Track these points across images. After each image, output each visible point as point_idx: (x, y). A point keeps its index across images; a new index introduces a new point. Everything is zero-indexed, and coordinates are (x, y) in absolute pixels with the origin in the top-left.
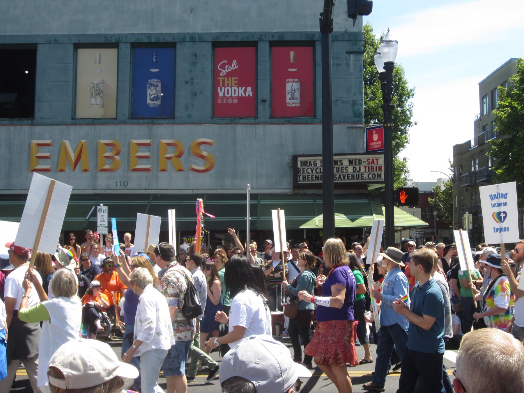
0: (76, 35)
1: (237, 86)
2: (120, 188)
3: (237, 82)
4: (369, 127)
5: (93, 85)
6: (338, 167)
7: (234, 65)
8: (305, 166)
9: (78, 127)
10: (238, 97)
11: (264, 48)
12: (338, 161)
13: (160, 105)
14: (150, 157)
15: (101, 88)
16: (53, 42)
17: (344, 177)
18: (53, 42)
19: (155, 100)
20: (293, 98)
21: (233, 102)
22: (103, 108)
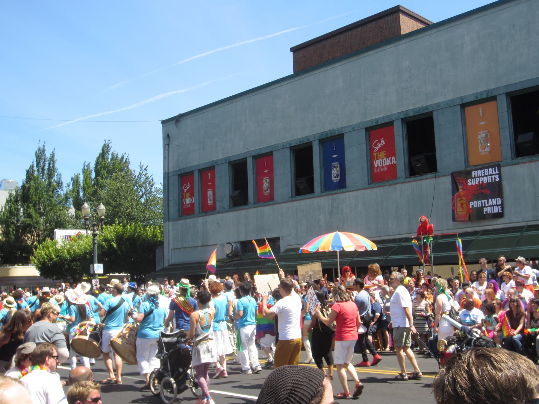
1: (385, 157)
3: (385, 154)
13: (340, 180)
20: (210, 200)
21: (384, 171)
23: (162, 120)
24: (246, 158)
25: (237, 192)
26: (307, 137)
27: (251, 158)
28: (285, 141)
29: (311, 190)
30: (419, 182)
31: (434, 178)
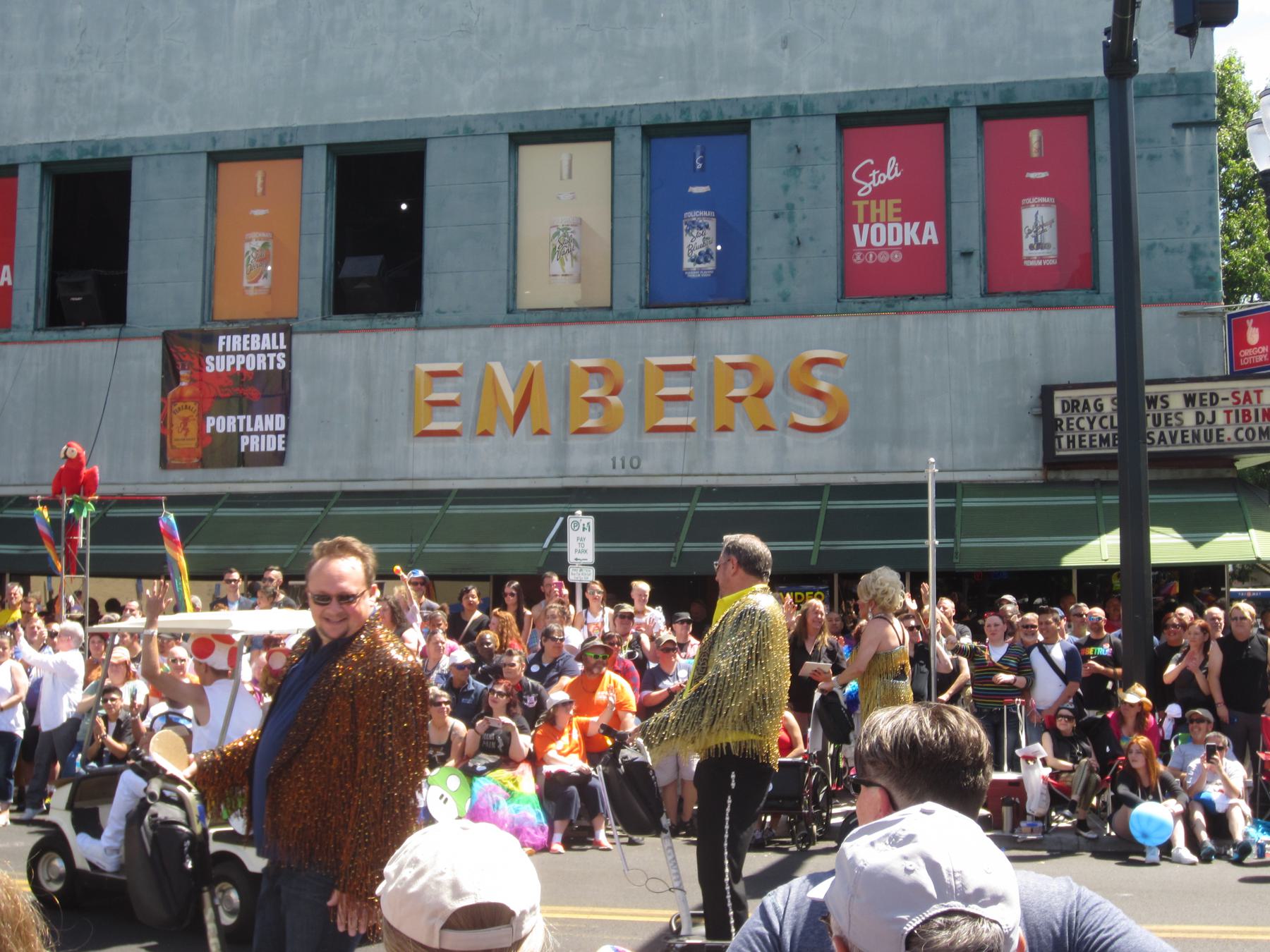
1: (900, 219)
2: (623, 472)
3: (899, 210)
4: (1233, 312)
5: (555, 230)
6: (1156, 413)
7: (893, 170)
8: (1073, 411)
9: (522, 331)
10: (903, 248)
11: (964, 124)
12: (1156, 397)
13: (716, 273)
14: (692, 396)
15: (573, 236)
16: (461, 132)
17: (1173, 439)
18: (461, 132)
19: (702, 260)
20: (1040, 246)
21: (890, 262)
22: (579, 285)
31: (409, 328)
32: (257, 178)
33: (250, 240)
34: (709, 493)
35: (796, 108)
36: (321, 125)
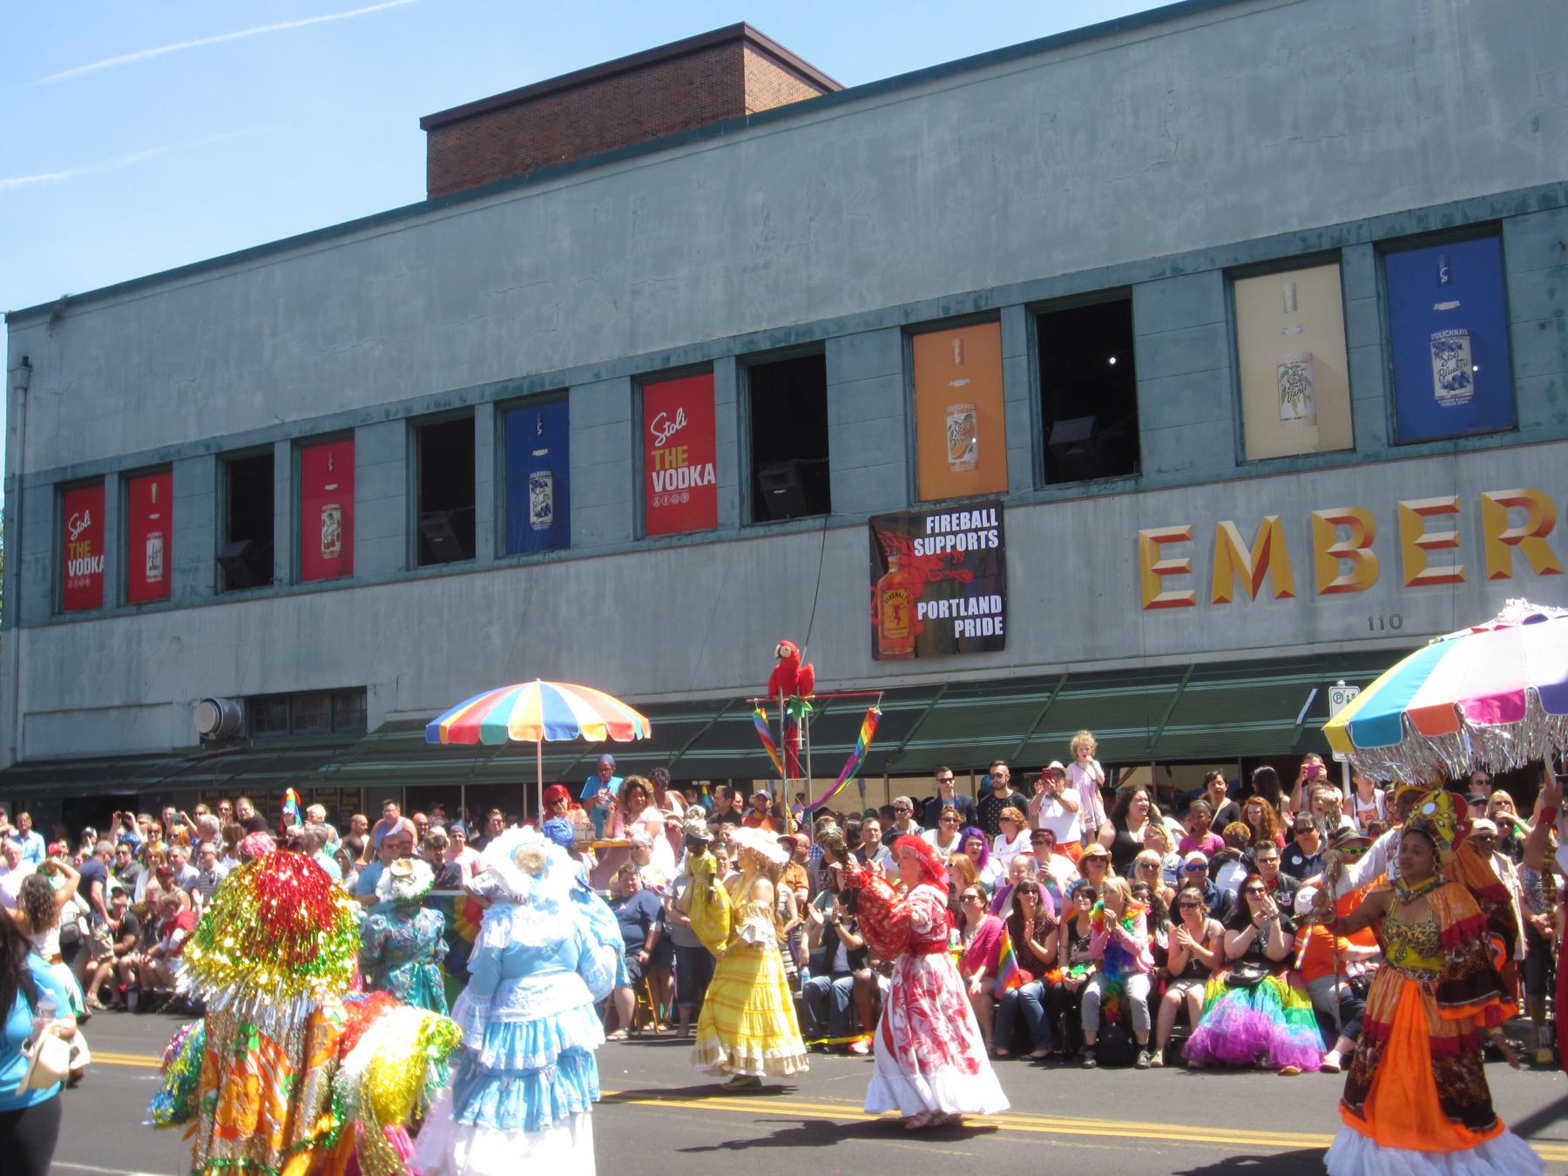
0: (1229, 246)
1: (686, 464)
2: (1382, 633)
3: (685, 456)
5: (1282, 369)
7: (681, 420)
9: (1253, 483)
20: (154, 567)
23: (7, 311)
24: (271, 445)
25: (241, 546)
26: (461, 393)
27: (288, 445)
28: (394, 399)
29: (466, 550)
30: (775, 540)
31: (819, 530)
32: (953, 349)
33: (952, 414)
34: (1204, 671)
35: (1556, 199)
36: (1018, 284)
